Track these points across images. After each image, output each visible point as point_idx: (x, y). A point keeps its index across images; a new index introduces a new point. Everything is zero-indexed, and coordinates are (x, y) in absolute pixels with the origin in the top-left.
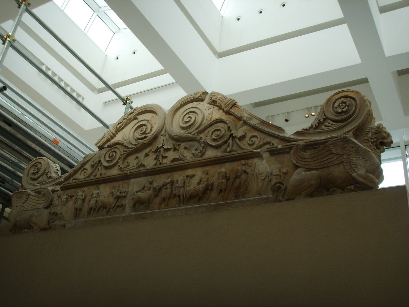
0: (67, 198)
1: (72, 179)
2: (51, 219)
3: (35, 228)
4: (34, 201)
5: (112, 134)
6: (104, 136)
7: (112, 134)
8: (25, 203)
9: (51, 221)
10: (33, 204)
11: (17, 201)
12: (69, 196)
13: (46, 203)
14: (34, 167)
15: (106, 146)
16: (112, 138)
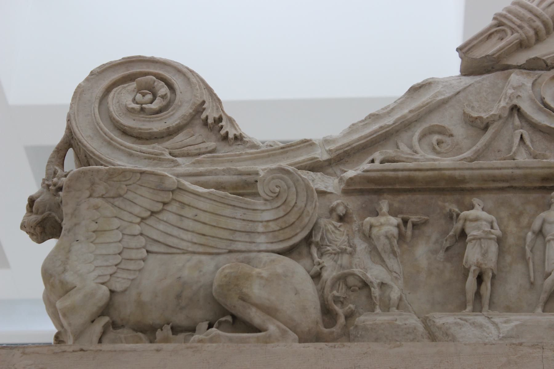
0: (398, 226)
1: (377, 156)
2: (337, 300)
3: (272, 328)
4: (203, 217)
5: (538, 23)
6: (500, 24)
7: (538, 23)
8: (150, 222)
9: (337, 308)
10: (206, 230)
11: (97, 208)
12: (405, 222)
13: (289, 233)
14: (133, 85)
15: (522, 58)
16: (538, 39)
